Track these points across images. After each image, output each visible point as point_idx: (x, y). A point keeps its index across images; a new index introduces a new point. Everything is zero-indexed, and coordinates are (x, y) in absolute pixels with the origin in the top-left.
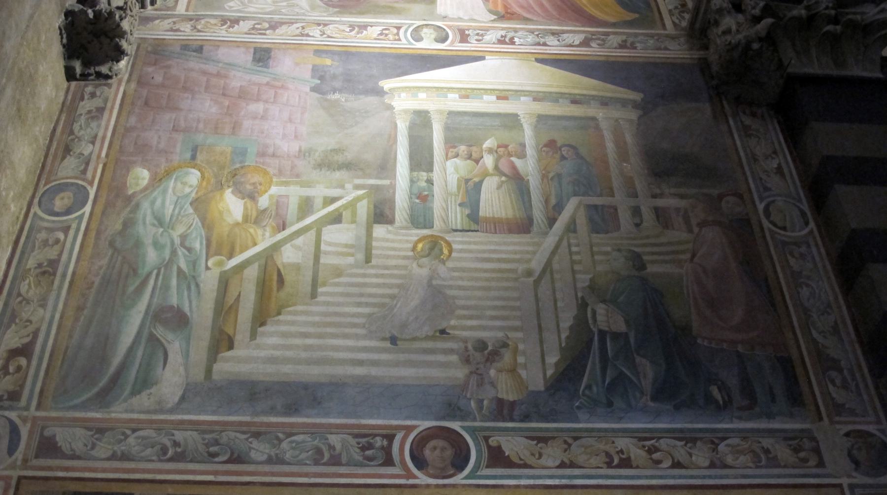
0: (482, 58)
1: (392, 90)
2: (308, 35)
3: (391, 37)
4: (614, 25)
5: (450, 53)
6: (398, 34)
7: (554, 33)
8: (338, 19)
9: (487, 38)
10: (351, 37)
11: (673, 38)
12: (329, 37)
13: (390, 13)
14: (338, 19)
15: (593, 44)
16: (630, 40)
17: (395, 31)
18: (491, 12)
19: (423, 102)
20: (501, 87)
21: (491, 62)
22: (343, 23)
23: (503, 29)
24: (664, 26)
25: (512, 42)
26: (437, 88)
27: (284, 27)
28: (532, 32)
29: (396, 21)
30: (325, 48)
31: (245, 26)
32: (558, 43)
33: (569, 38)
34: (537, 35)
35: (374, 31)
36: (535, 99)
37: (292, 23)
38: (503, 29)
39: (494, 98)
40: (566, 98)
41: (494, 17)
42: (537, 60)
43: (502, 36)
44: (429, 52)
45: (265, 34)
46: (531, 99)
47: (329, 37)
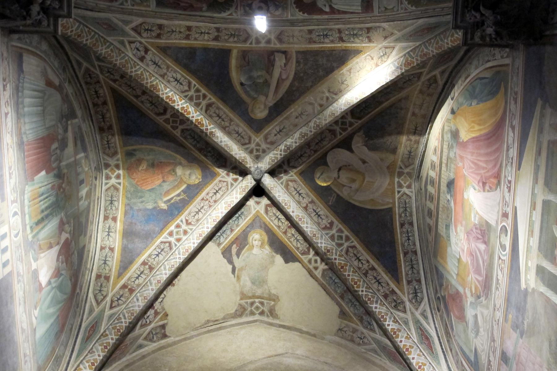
0: (516, 208)
1: (526, 284)
2: (499, 320)
3: (503, 266)
4: (506, 102)
5: (512, 229)
6: (502, 260)
7: (508, 150)
8: (493, 295)
9: (507, 199)
10: (501, 291)
11: (513, 61)
12: (500, 307)
13: (493, 258)
14: (493, 295)
15: (514, 123)
16: (513, 94)
17: (500, 260)
18: (496, 189)
19: (533, 264)
20: (530, 205)
21: (518, 204)
22: (495, 293)
23: (504, 185)
24: (507, 65)
25: (510, 182)
26: (527, 251)
27: (494, 333)
28: (506, 165)
29: (496, 258)
30: (505, 313)
31: (492, 359)
32: (512, 149)
33: (510, 140)
34: (508, 162)
35: (500, 277)
36: (537, 183)
37: (493, 326)
38: (504, 185)
39: (534, 212)
40: (538, 158)
41: (498, 189)
42: (519, 169)
43: (507, 188)
44: (511, 244)
45: (496, 348)
46: (536, 185)
47: (500, 307)
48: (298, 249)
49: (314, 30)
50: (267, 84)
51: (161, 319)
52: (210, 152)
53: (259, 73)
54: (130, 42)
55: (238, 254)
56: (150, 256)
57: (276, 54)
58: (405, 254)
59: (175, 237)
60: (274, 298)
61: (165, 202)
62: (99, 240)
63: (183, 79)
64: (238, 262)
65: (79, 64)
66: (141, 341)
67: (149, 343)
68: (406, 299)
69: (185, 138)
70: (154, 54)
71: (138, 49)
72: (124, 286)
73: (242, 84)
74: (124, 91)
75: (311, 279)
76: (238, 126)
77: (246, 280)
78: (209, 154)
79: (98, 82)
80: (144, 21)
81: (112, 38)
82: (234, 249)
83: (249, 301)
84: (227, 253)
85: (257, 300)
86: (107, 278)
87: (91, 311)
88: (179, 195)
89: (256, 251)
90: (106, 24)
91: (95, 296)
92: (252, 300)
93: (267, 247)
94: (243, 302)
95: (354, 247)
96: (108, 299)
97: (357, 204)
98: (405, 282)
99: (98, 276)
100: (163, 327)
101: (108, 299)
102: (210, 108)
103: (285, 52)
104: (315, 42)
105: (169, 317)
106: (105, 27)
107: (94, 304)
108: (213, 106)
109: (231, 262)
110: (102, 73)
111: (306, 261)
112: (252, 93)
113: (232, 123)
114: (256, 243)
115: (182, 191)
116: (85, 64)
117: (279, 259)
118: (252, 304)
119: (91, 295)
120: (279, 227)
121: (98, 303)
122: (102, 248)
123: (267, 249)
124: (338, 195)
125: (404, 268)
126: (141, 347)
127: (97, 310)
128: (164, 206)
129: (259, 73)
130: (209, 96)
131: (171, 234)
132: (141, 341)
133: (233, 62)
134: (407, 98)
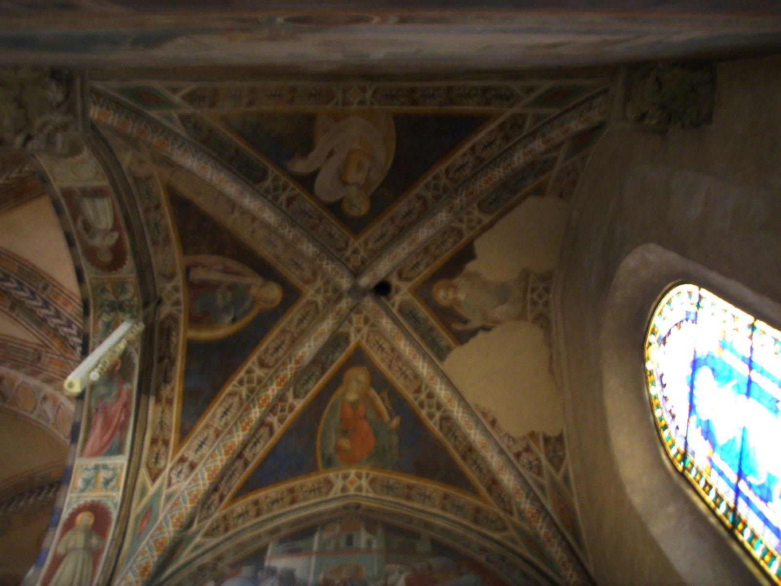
48: (455, 242)
49: (152, 239)
50: (232, 288)
51: (537, 443)
52: (327, 357)
53: (220, 296)
54: (170, 484)
55: (465, 321)
56: (456, 448)
57: (191, 278)
58: (451, 102)
59: (434, 410)
60: (525, 274)
61: (392, 418)
62: (433, 510)
63: (224, 404)
64: (475, 322)
65: (197, 547)
66: (559, 477)
67: (564, 464)
68: (510, 112)
69: (306, 392)
70: (189, 448)
71: (180, 472)
72: (489, 490)
73: (234, 320)
74: (237, 482)
75: (496, 227)
76: (291, 321)
77: (499, 312)
78: (330, 358)
79: (225, 518)
80: (145, 466)
81: (160, 512)
82: (457, 327)
83: (529, 308)
84: (462, 338)
85: (529, 296)
86: (478, 510)
87: (512, 540)
88: (383, 400)
89: (462, 296)
90: (143, 521)
91: (497, 530)
92: (529, 304)
93: (456, 281)
94: (530, 317)
95: (447, 171)
96: (502, 514)
97: (391, 161)
98: (488, 109)
99: (475, 521)
100: (547, 440)
101: (502, 514)
102: (266, 361)
103: (188, 270)
104: (168, 236)
105: (536, 430)
106: (145, 523)
107: (506, 534)
108: (263, 357)
109: (473, 333)
110: (211, 516)
111: (472, 233)
112: (247, 304)
113: (288, 328)
114: (451, 295)
115: (379, 394)
116: (198, 539)
117: (471, 267)
118: (534, 303)
119: (497, 536)
120: (428, 265)
121: (504, 528)
122: (444, 508)
123: (459, 281)
124: (382, 185)
125: (471, 107)
126: (566, 478)
127: (512, 532)
128: (395, 422)
129: (220, 296)
130: (249, 365)
131: (431, 416)
132: (559, 477)
133: (205, 335)
134: (225, 120)
